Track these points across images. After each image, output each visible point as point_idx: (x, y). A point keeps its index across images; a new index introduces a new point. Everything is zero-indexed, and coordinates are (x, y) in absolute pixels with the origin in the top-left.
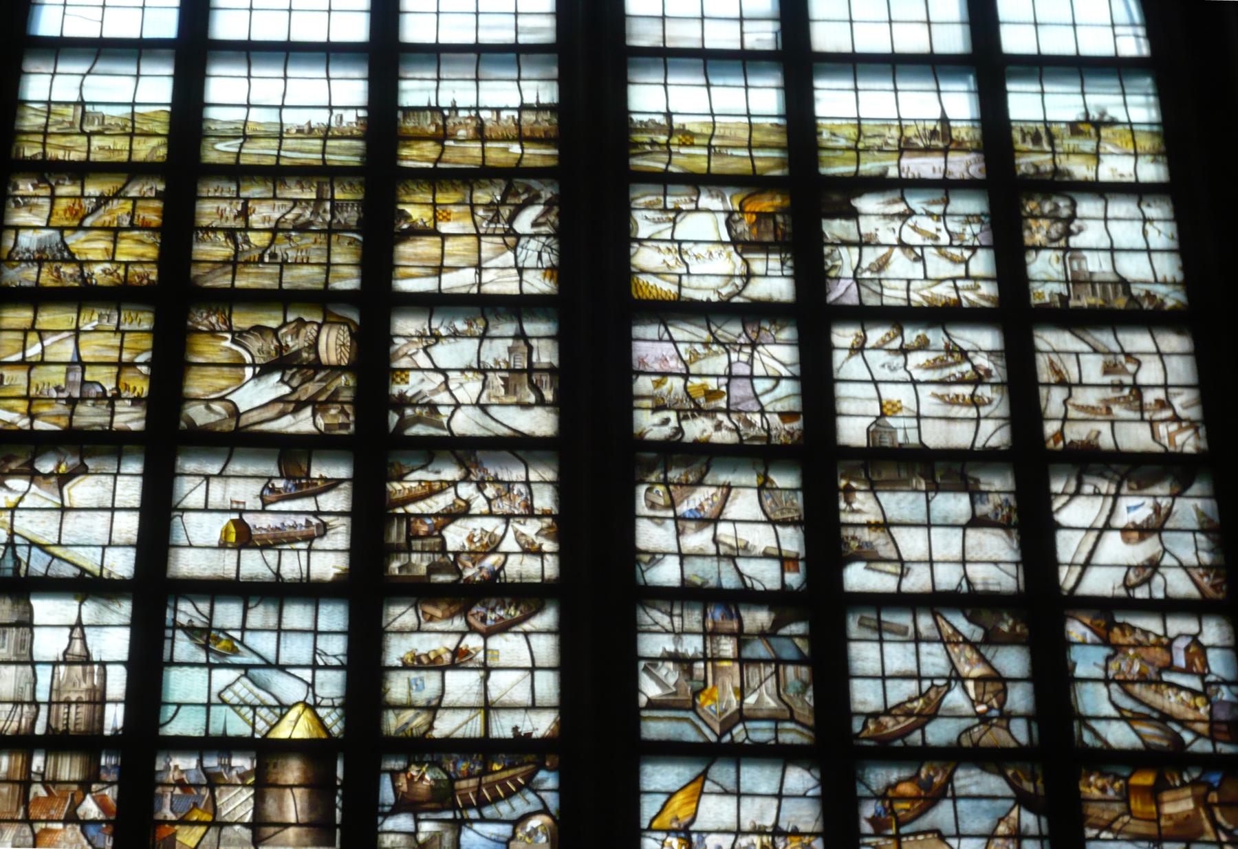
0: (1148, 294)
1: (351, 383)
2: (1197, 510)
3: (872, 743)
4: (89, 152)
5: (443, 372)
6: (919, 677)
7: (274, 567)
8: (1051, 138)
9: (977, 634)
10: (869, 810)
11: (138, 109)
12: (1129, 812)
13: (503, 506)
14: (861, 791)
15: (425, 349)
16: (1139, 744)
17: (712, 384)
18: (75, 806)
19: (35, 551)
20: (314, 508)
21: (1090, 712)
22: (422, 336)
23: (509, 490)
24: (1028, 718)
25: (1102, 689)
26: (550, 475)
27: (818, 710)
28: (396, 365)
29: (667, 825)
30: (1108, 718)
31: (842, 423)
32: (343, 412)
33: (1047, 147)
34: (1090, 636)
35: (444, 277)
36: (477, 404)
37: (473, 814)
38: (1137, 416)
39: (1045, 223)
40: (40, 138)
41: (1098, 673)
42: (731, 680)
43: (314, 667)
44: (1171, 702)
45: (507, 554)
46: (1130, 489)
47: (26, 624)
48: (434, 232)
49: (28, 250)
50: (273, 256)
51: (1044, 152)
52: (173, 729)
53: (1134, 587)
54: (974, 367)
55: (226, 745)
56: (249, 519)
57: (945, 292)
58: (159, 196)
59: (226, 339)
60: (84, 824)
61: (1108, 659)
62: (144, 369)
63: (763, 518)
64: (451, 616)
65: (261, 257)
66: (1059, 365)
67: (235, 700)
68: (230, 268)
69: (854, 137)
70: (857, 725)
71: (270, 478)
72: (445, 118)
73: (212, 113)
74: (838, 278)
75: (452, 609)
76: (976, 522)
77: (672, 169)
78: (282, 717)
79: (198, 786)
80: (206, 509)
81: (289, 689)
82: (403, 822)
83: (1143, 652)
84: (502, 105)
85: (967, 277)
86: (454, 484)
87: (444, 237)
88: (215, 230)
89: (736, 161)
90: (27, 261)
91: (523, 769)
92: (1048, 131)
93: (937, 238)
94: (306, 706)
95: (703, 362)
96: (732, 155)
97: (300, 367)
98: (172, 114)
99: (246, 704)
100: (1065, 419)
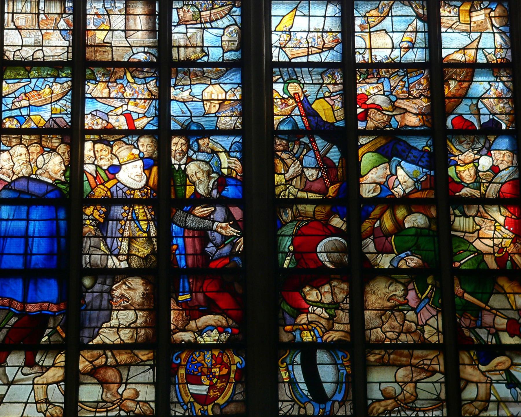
10: (358, 22)
37: (208, 25)
60: (60, 30)
79: (104, 15)
82: (182, 28)
91: (228, 7)
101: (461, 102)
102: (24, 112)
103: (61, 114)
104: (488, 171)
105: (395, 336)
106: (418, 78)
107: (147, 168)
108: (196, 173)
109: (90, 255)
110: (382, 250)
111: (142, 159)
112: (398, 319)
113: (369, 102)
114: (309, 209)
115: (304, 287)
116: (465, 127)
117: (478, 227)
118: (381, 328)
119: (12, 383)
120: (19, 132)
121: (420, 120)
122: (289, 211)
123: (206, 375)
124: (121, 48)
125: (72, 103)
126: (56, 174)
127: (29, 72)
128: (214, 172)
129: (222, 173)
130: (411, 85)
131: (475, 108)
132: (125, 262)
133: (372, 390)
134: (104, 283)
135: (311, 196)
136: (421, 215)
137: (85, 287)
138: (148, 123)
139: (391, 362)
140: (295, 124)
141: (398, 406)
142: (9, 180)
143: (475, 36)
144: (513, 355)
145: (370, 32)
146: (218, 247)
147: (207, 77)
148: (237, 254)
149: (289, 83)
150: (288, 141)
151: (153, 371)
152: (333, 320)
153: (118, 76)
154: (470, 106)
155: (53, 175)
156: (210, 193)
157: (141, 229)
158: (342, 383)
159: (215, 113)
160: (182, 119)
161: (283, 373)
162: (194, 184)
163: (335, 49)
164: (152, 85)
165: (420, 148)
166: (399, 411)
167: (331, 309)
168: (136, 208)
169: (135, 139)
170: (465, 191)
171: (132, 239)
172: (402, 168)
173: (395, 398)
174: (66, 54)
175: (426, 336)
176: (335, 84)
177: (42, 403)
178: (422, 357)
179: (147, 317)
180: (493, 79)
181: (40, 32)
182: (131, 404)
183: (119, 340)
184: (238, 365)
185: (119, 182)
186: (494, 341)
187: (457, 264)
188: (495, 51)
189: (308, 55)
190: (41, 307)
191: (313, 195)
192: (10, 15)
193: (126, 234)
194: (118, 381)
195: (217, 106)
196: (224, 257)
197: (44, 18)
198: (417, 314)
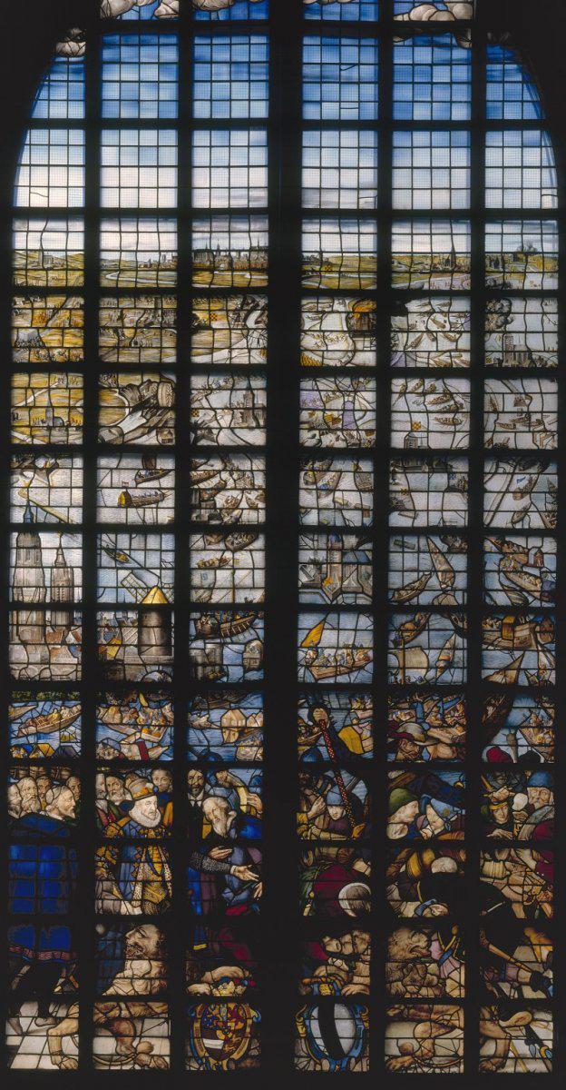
0: (541, 359)
1: (173, 416)
3: (396, 604)
4: (47, 280)
5: (214, 409)
6: (418, 571)
7: (142, 517)
8: (504, 262)
9: (444, 548)
10: (393, 636)
11: (69, 253)
12: (502, 637)
13: (241, 484)
15: (206, 396)
16: (510, 604)
17: (336, 414)
18: (65, 637)
19: (39, 509)
20: (158, 486)
23: (244, 475)
26: (262, 467)
27: (374, 588)
28: (193, 406)
30: (497, 590)
31: (394, 435)
32: (170, 433)
33: (501, 270)
34: (494, 549)
35: (215, 354)
36: (230, 428)
37: (228, 640)
38: (527, 429)
39: (495, 316)
41: (496, 568)
42: (338, 574)
43: (161, 568)
44: (525, 582)
45: (243, 509)
46: (520, 470)
47: (38, 547)
48: (209, 328)
50: (136, 343)
51: (500, 272)
52: (103, 600)
56: (130, 491)
57: (445, 358)
58: (82, 307)
59: (116, 392)
60: (69, 646)
61: (501, 560)
62: (80, 410)
63: (355, 489)
64: (219, 542)
65: (130, 344)
67: (128, 585)
68: (116, 351)
69: (409, 264)
71: (139, 469)
72: (214, 257)
73: (104, 255)
74: (397, 351)
75: (220, 538)
76: (450, 489)
78: (148, 593)
79: (115, 627)
80: (112, 488)
81: (151, 580)
82: (199, 644)
83: (515, 556)
85: (456, 350)
86: (219, 472)
87: (214, 330)
88: (108, 328)
89: (350, 283)
90: (24, 347)
92: (503, 257)
93: (444, 327)
94: (158, 588)
97: (150, 408)
98: (85, 256)
102: (32, 740)
105: (415, 990)
106: (454, 702)
107: (161, 805)
108: (213, 811)
109: (103, 900)
110: (407, 897)
111: (156, 793)
113: (401, 730)
114: (333, 851)
115: (325, 937)
117: (508, 873)
118: (402, 981)
119: (27, 1034)
120: (26, 763)
121: (453, 752)
122: (311, 854)
123: (223, 1030)
124: (133, 667)
125: (83, 728)
126: (66, 810)
128: (232, 810)
130: (446, 712)
131: (511, 738)
132: (139, 908)
133: (389, 1045)
136: (449, 859)
141: (416, 1062)
142: (16, 816)
143: (517, 654)
144: (534, 1010)
145: (404, 649)
146: (236, 892)
147: (226, 700)
148: (255, 901)
151: (168, 1023)
153: (130, 698)
154: (507, 736)
155: (63, 811)
157: (155, 873)
160: (199, 749)
161: (300, 1028)
162: (211, 822)
164: (167, 710)
165: (452, 783)
166: (415, 1068)
168: (150, 849)
169: (149, 771)
170: (497, 832)
171: (146, 883)
172: (432, 806)
173: (412, 1054)
174: (75, 673)
175: (448, 990)
176: (365, 709)
178: (443, 1012)
179: (161, 968)
180: (533, 705)
181: (46, 648)
182: (145, 1058)
183: (133, 992)
185: (132, 819)
186: (516, 996)
189: (336, 676)
191: (337, 836)
192: (15, 628)
193: (140, 877)
195: (237, 735)
196: (238, 903)
197: (51, 631)
198: (439, 966)
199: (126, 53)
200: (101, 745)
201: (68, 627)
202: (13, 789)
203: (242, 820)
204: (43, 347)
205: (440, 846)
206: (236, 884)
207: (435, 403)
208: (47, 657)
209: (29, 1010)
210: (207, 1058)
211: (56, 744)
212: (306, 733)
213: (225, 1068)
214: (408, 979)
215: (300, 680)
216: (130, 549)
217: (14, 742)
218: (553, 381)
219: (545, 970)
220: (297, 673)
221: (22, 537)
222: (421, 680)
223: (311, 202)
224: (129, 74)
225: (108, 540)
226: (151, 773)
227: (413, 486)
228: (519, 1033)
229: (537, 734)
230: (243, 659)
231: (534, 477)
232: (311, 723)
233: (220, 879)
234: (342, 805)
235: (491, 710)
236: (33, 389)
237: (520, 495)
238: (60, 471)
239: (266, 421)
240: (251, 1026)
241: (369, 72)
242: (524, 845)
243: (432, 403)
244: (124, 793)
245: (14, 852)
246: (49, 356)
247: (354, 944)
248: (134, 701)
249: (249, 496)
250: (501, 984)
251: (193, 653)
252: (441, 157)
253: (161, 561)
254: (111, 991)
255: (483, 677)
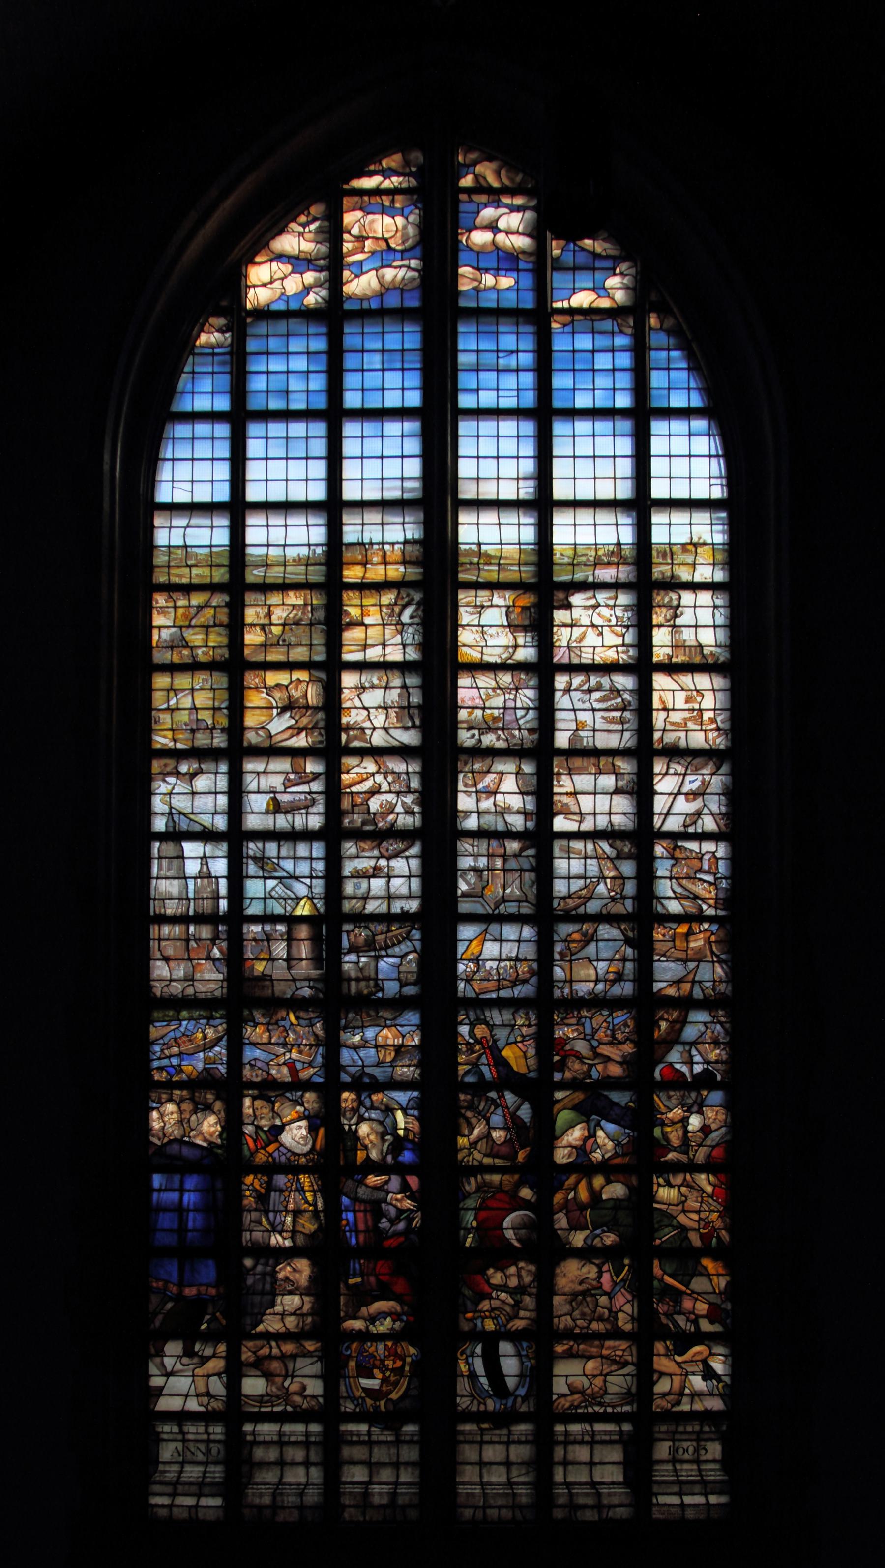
1: (324, 717)
2: (722, 781)
3: (562, 913)
4: (191, 577)
5: (366, 709)
6: (585, 878)
10: (558, 948)
11: (214, 549)
12: (674, 947)
14: (556, 938)
15: (358, 696)
17: (496, 713)
18: (210, 951)
19: (182, 817)
21: (662, 895)
22: (356, 688)
23: (399, 778)
24: (633, 898)
25: (668, 882)
26: (418, 769)
27: (539, 896)
29: (469, 957)
33: (669, 561)
34: (665, 854)
35: (367, 651)
37: (383, 953)
38: (699, 728)
39: (664, 610)
40: (166, 570)
41: (667, 874)
44: (699, 889)
45: (398, 814)
47: (181, 857)
48: (362, 624)
49: (166, 641)
50: (284, 641)
51: (668, 564)
52: (250, 911)
53: (688, 826)
54: (623, 700)
55: (274, 919)
56: (279, 797)
58: (227, 605)
60: (214, 960)
61: (673, 866)
62: (225, 711)
63: (518, 791)
64: (372, 849)
65: (278, 642)
66: (664, 699)
67: (277, 896)
69: (572, 556)
70: (555, 903)
71: (287, 773)
72: (366, 550)
76: (617, 791)
77: (480, 580)
78: (298, 904)
79: (262, 940)
80: (259, 792)
81: (301, 889)
82: (352, 957)
84: (395, 541)
85: (623, 645)
86: (373, 774)
87: (366, 626)
88: (255, 625)
90: (166, 647)
92: (671, 549)
93: (610, 621)
94: (309, 898)
95: (492, 700)
96: (511, 570)
97: (299, 708)
99: (282, 898)
100: (664, 730)
101: (671, 1049)
102: (175, 1061)
103: (214, 1063)
104: (698, 1131)
105: (585, 1325)
107: (312, 1130)
108: (368, 1135)
109: (251, 1231)
110: (575, 1226)
112: (591, 1306)
113: (568, 1047)
114: (496, 1178)
115: (488, 1269)
116: (675, 1079)
117: (683, 1199)
118: (571, 1315)
120: (169, 1085)
121: (624, 1070)
122: (472, 1180)
125: (228, 1049)
127: (179, 1013)
128: (388, 1134)
129: (399, 1135)
131: (687, 1055)
132: (290, 1240)
134: (266, 1264)
135: (498, 1162)
137: (245, 1267)
138: (314, 1074)
139: (580, 1353)
140: (481, 1075)
141: (585, 1401)
142: (159, 1143)
143: (692, 965)
144: (712, 1344)
145: (571, 961)
146: (393, 1222)
147: (382, 1017)
149: (476, 1025)
150: (473, 1096)
151: (321, 1363)
152: (518, 1306)
154: (682, 1053)
155: (208, 1137)
156: (384, 1158)
158: (526, 1376)
159: (390, 1062)
160: (353, 1070)
161: (462, 1366)
162: (366, 1148)
163: (530, 982)
165: (623, 1104)
166: (586, 1407)
167: (516, 1294)
169: (299, 1093)
170: (671, 1156)
171: (297, 1213)
173: (582, 1392)
175: (620, 1324)
176: (529, 1026)
177: (203, 1396)
178: (614, 1347)
179: (313, 1303)
181: (190, 965)
182: (297, 1399)
183: (284, 1328)
184: (414, 1357)
185: (282, 1145)
186: (693, 1329)
187: (658, 1242)
188: (714, 985)
189: (498, 990)
190: (199, 1290)
192: (157, 942)
193: (291, 1206)
194: (283, 1373)
195: (393, 1054)
196: (397, 1234)
197: (195, 945)
198: (610, 1299)
199: (274, 344)
200: (248, 1066)
201: (213, 941)
202: (155, 1114)
203: (398, 1145)
204: (187, 646)
205: (607, 1169)
206: (393, 1212)
207: (601, 700)
208: (191, 973)
209: (173, 1348)
210: (363, 1398)
211: (200, 1066)
212: (467, 1051)
213: (383, 1409)
214: (576, 1314)
215: (460, 995)
216: (278, 858)
217: (156, 1064)
218: (725, 677)
219: (723, 1302)
220: (456, 987)
221: (164, 846)
222: (590, 994)
223: (467, 492)
224: (277, 365)
225: (255, 848)
226: (302, 1096)
227: (579, 788)
228: (696, 1369)
229: (712, 1051)
230: (399, 973)
231: (707, 778)
232: (471, 1041)
233: (375, 1208)
234: (506, 1128)
235: (664, 1025)
236: (175, 690)
237: (691, 797)
238: (204, 776)
239: (422, 721)
240: (411, 1364)
241: (527, 359)
242: (700, 1169)
243: (597, 701)
244: (273, 1117)
245: (157, 1180)
246: (192, 656)
247: (519, 1276)
248: (283, 1019)
249: (404, 799)
250: (675, 1317)
251: (346, 967)
252: (605, 446)
253: (311, 869)
254: (261, 1328)
255: (655, 990)
